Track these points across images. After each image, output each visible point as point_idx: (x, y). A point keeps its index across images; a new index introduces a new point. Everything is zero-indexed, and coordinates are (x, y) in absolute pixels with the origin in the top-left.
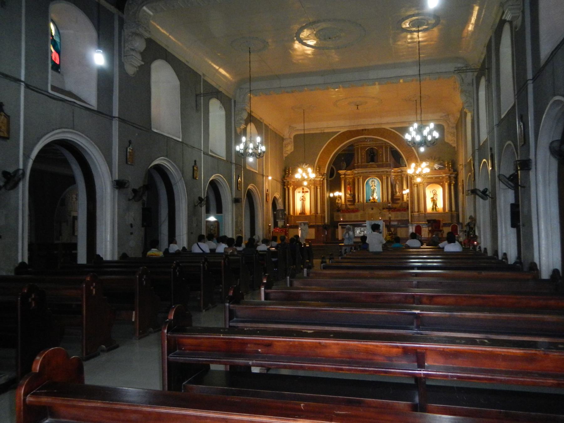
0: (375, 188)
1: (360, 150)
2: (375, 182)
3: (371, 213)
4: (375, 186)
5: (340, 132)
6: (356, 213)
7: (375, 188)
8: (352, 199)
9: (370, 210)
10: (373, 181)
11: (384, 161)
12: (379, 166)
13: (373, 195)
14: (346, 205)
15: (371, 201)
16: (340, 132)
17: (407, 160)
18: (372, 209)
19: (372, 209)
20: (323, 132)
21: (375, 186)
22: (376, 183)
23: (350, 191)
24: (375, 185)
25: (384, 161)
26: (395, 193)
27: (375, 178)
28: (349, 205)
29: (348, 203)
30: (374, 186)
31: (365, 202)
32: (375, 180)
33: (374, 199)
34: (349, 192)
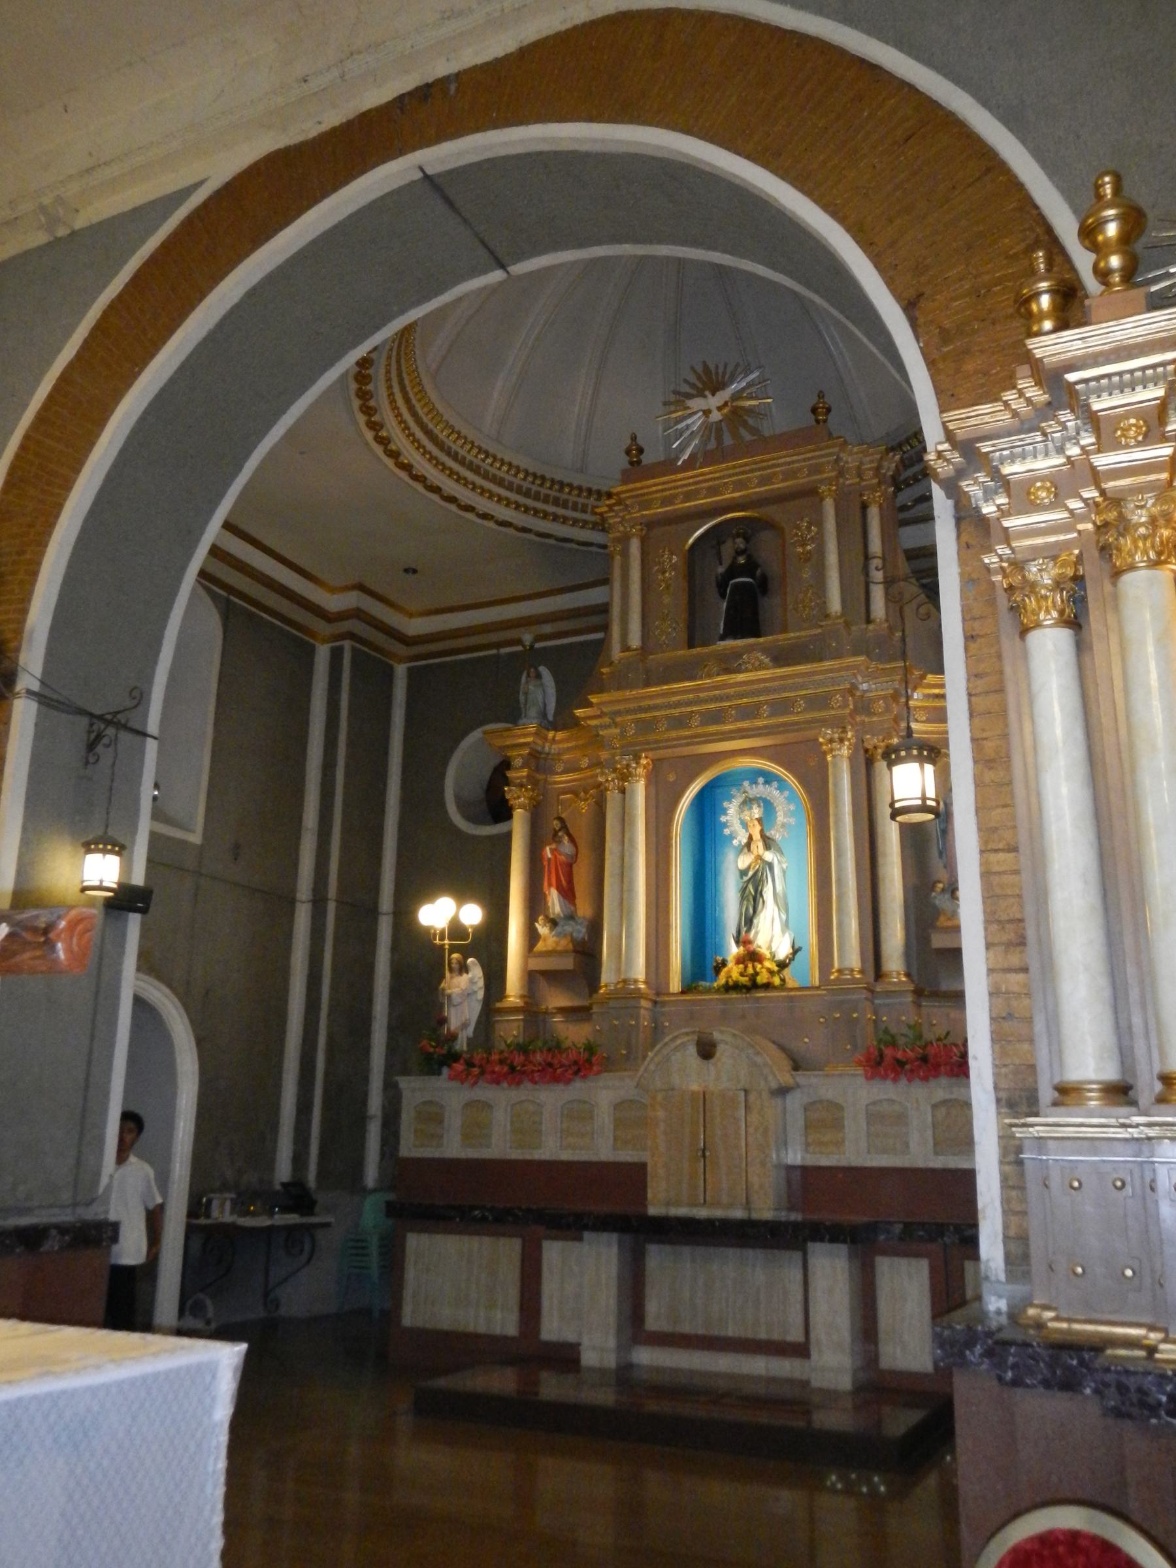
0: (769, 856)
1: (635, 547)
2: (768, 806)
3: (695, 1087)
4: (768, 843)
5: (202, 183)
6: (578, 1090)
7: (769, 856)
8: (567, 963)
9: (692, 1050)
10: (748, 802)
11: (835, 604)
12: (780, 658)
13: (749, 922)
14: (531, 1010)
15: (722, 979)
16: (202, 183)
17: (910, 307)
18: (706, 1050)
19: (706, 1050)
20: (62, 232)
21: (768, 843)
22: (781, 818)
23: (568, 893)
24: (773, 833)
25: (835, 604)
26: (941, 901)
27: (769, 778)
28: (562, 1010)
29: (556, 999)
30: (758, 846)
31: (675, 985)
32: (772, 792)
33: (753, 957)
34: (554, 902)
